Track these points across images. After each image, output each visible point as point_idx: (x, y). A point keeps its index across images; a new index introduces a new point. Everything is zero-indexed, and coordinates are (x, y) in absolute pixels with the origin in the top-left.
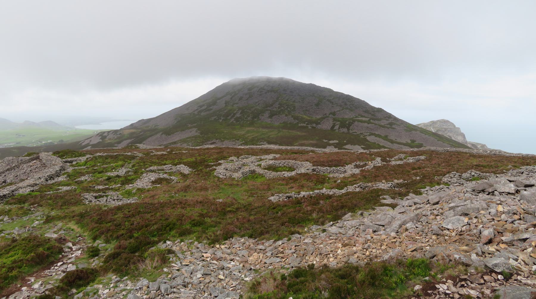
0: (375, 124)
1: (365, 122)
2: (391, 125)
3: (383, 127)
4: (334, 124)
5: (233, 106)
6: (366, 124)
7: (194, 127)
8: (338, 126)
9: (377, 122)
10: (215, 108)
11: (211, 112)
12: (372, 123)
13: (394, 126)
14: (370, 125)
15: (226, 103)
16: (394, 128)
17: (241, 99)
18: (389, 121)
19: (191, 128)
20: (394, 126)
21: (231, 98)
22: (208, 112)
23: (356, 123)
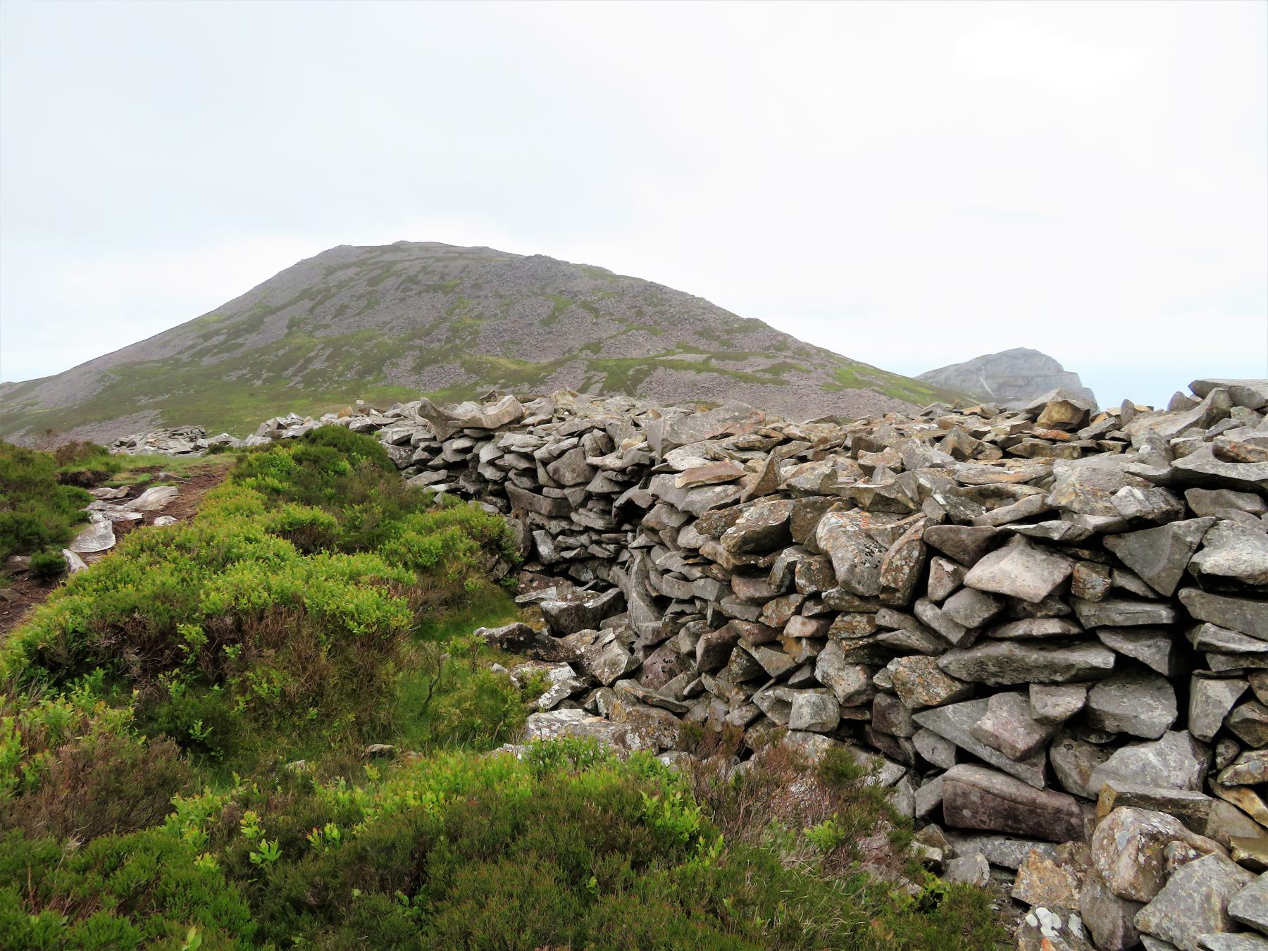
0: (722, 372)
1: (688, 367)
2: (777, 374)
3: (746, 379)
4: (589, 379)
5: (311, 334)
6: (690, 375)
7: (156, 406)
8: (600, 385)
9: (730, 365)
10: (252, 340)
11: (238, 353)
12: (713, 370)
13: (785, 376)
14: (704, 374)
15: (289, 327)
16: (782, 383)
17: (341, 311)
18: (776, 361)
19: (142, 408)
20: (785, 376)
21: (311, 310)
22: (226, 356)
23: (660, 372)
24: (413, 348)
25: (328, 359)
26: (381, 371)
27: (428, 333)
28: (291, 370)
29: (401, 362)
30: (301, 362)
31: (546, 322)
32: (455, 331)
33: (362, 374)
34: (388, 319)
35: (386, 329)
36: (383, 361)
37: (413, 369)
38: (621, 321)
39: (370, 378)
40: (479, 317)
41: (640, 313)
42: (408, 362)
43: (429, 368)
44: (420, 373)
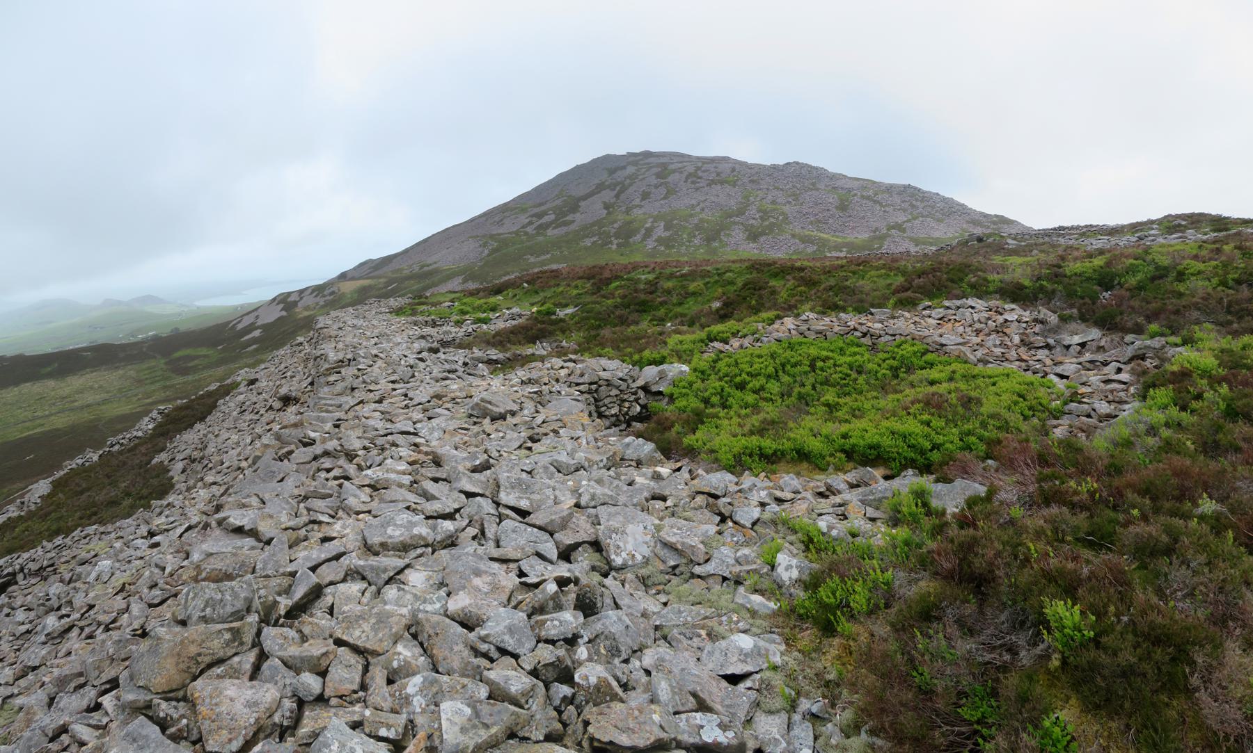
24: (736, 223)
25: (667, 228)
26: (721, 241)
27: (741, 213)
28: (638, 237)
29: (733, 233)
30: (643, 231)
31: (843, 207)
32: (765, 214)
33: (709, 240)
34: (694, 202)
35: (698, 209)
36: (718, 232)
37: (748, 239)
38: (905, 210)
39: (716, 244)
40: (774, 202)
41: (913, 206)
42: (738, 234)
43: (762, 239)
44: (755, 242)
